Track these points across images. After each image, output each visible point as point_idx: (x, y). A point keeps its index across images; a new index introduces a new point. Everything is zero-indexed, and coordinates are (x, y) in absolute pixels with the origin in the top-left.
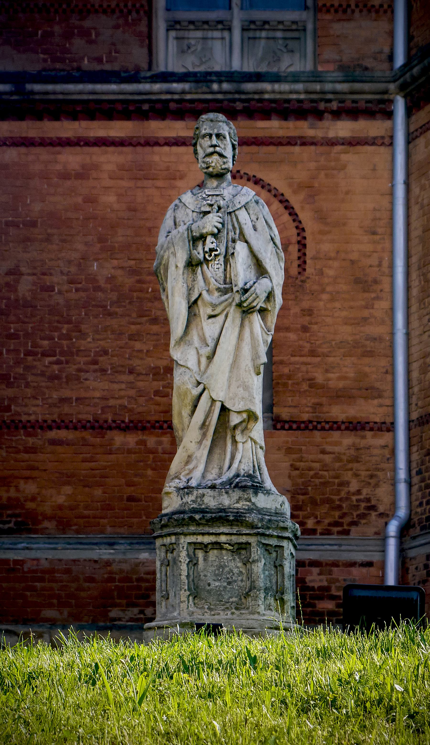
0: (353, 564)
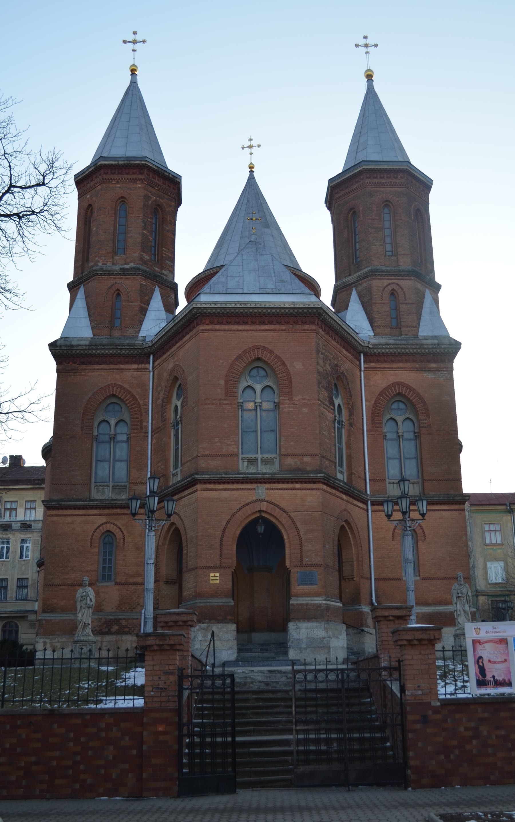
0: (134, 619)
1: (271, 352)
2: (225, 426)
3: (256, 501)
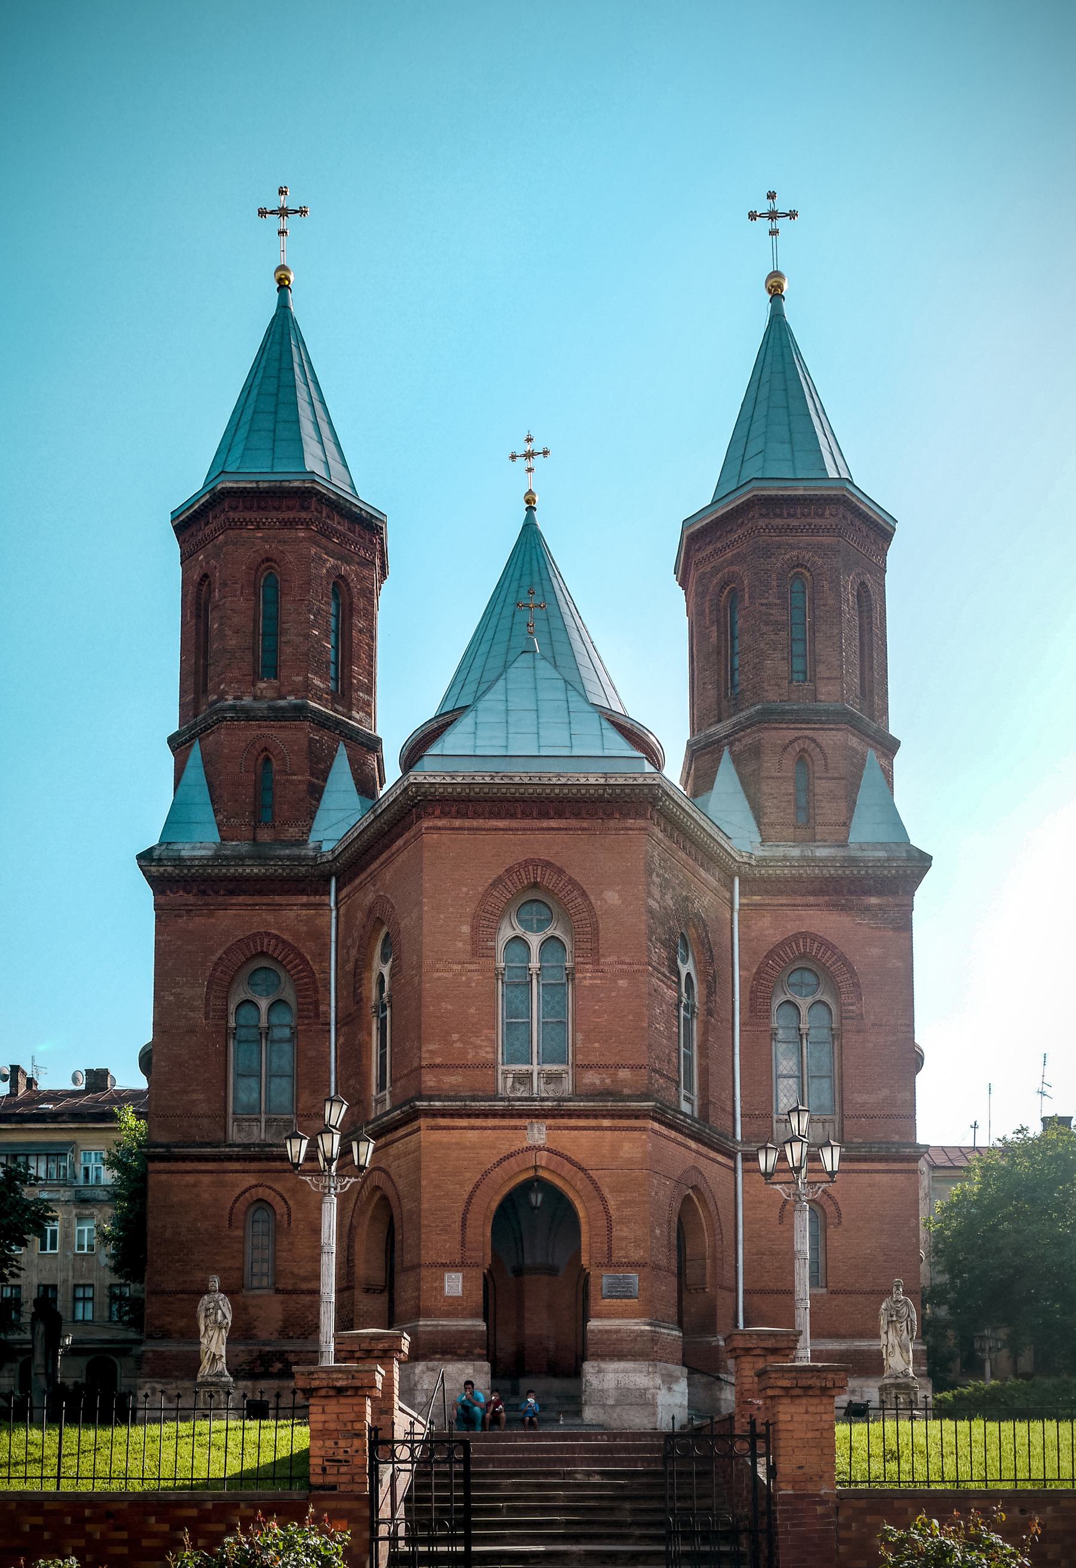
1: (560, 871)
3: (529, 1149)
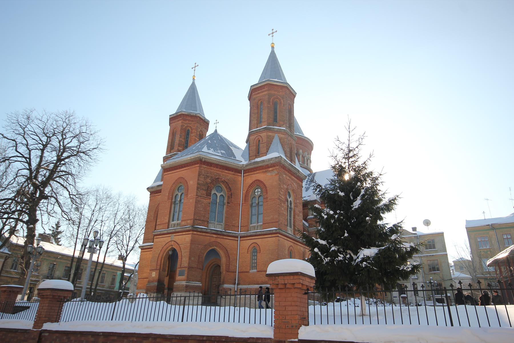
1: (184, 179)
2: (166, 211)
3: (170, 241)
